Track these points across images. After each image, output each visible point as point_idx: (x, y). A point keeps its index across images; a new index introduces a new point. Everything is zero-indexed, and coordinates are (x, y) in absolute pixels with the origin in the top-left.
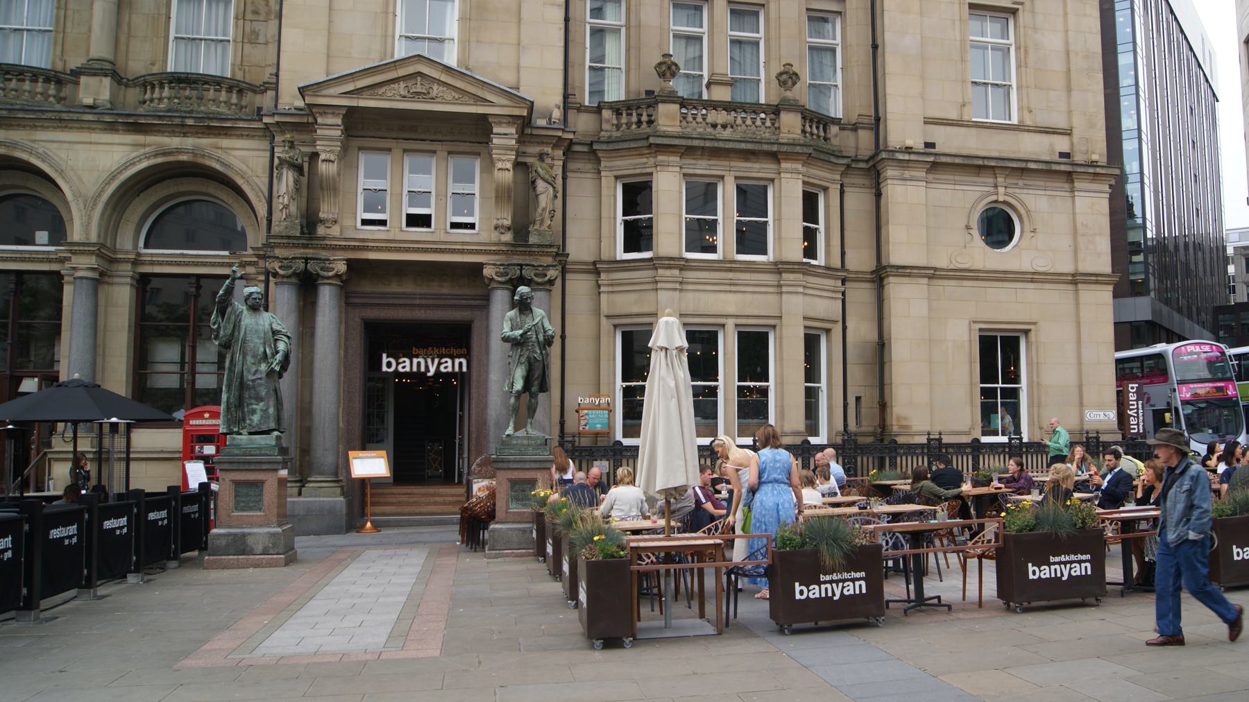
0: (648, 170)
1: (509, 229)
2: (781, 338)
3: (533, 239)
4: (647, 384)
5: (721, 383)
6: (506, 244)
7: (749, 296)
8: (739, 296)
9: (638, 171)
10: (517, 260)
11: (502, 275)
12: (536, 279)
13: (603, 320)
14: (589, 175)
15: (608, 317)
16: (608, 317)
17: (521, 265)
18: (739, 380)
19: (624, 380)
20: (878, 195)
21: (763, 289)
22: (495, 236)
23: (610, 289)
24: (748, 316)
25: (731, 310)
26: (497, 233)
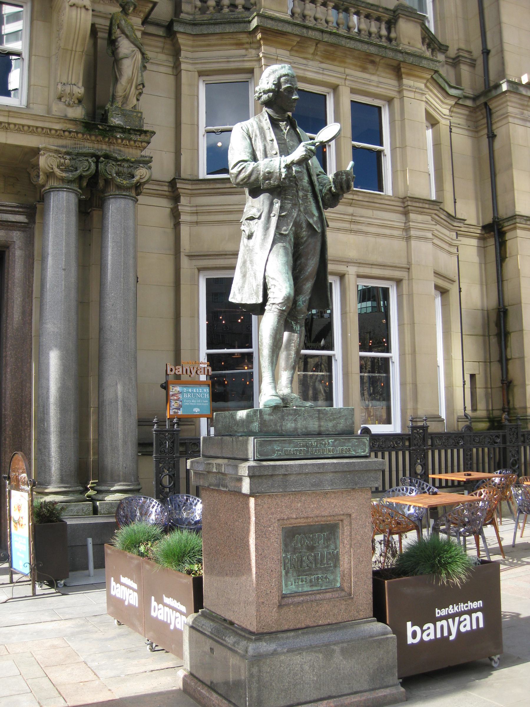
0: (247, 65)
1: (80, 101)
2: (411, 295)
3: (116, 121)
4: (253, 350)
5: (337, 352)
6: (74, 121)
7: (371, 239)
8: (360, 238)
9: (233, 66)
10: (90, 145)
11: (67, 170)
12: (119, 180)
13: (185, 262)
14: (162, 69)
15: (191, 257)
16: (191, 257)
17: (98, 157)
18: (363, 347)
19: (209, 347)
20: (492, 137)
21: (387, 232)
22: (58, 108)
23: (194, 218)
24: (372, 265)
25: (352, 254)
26: (61, 106)
